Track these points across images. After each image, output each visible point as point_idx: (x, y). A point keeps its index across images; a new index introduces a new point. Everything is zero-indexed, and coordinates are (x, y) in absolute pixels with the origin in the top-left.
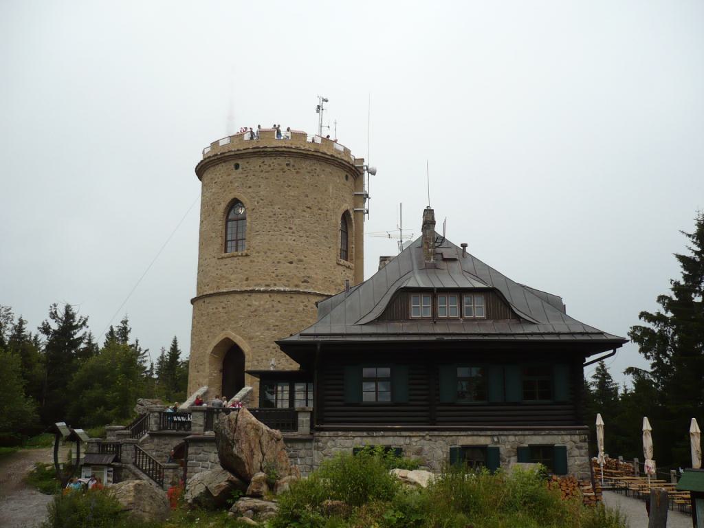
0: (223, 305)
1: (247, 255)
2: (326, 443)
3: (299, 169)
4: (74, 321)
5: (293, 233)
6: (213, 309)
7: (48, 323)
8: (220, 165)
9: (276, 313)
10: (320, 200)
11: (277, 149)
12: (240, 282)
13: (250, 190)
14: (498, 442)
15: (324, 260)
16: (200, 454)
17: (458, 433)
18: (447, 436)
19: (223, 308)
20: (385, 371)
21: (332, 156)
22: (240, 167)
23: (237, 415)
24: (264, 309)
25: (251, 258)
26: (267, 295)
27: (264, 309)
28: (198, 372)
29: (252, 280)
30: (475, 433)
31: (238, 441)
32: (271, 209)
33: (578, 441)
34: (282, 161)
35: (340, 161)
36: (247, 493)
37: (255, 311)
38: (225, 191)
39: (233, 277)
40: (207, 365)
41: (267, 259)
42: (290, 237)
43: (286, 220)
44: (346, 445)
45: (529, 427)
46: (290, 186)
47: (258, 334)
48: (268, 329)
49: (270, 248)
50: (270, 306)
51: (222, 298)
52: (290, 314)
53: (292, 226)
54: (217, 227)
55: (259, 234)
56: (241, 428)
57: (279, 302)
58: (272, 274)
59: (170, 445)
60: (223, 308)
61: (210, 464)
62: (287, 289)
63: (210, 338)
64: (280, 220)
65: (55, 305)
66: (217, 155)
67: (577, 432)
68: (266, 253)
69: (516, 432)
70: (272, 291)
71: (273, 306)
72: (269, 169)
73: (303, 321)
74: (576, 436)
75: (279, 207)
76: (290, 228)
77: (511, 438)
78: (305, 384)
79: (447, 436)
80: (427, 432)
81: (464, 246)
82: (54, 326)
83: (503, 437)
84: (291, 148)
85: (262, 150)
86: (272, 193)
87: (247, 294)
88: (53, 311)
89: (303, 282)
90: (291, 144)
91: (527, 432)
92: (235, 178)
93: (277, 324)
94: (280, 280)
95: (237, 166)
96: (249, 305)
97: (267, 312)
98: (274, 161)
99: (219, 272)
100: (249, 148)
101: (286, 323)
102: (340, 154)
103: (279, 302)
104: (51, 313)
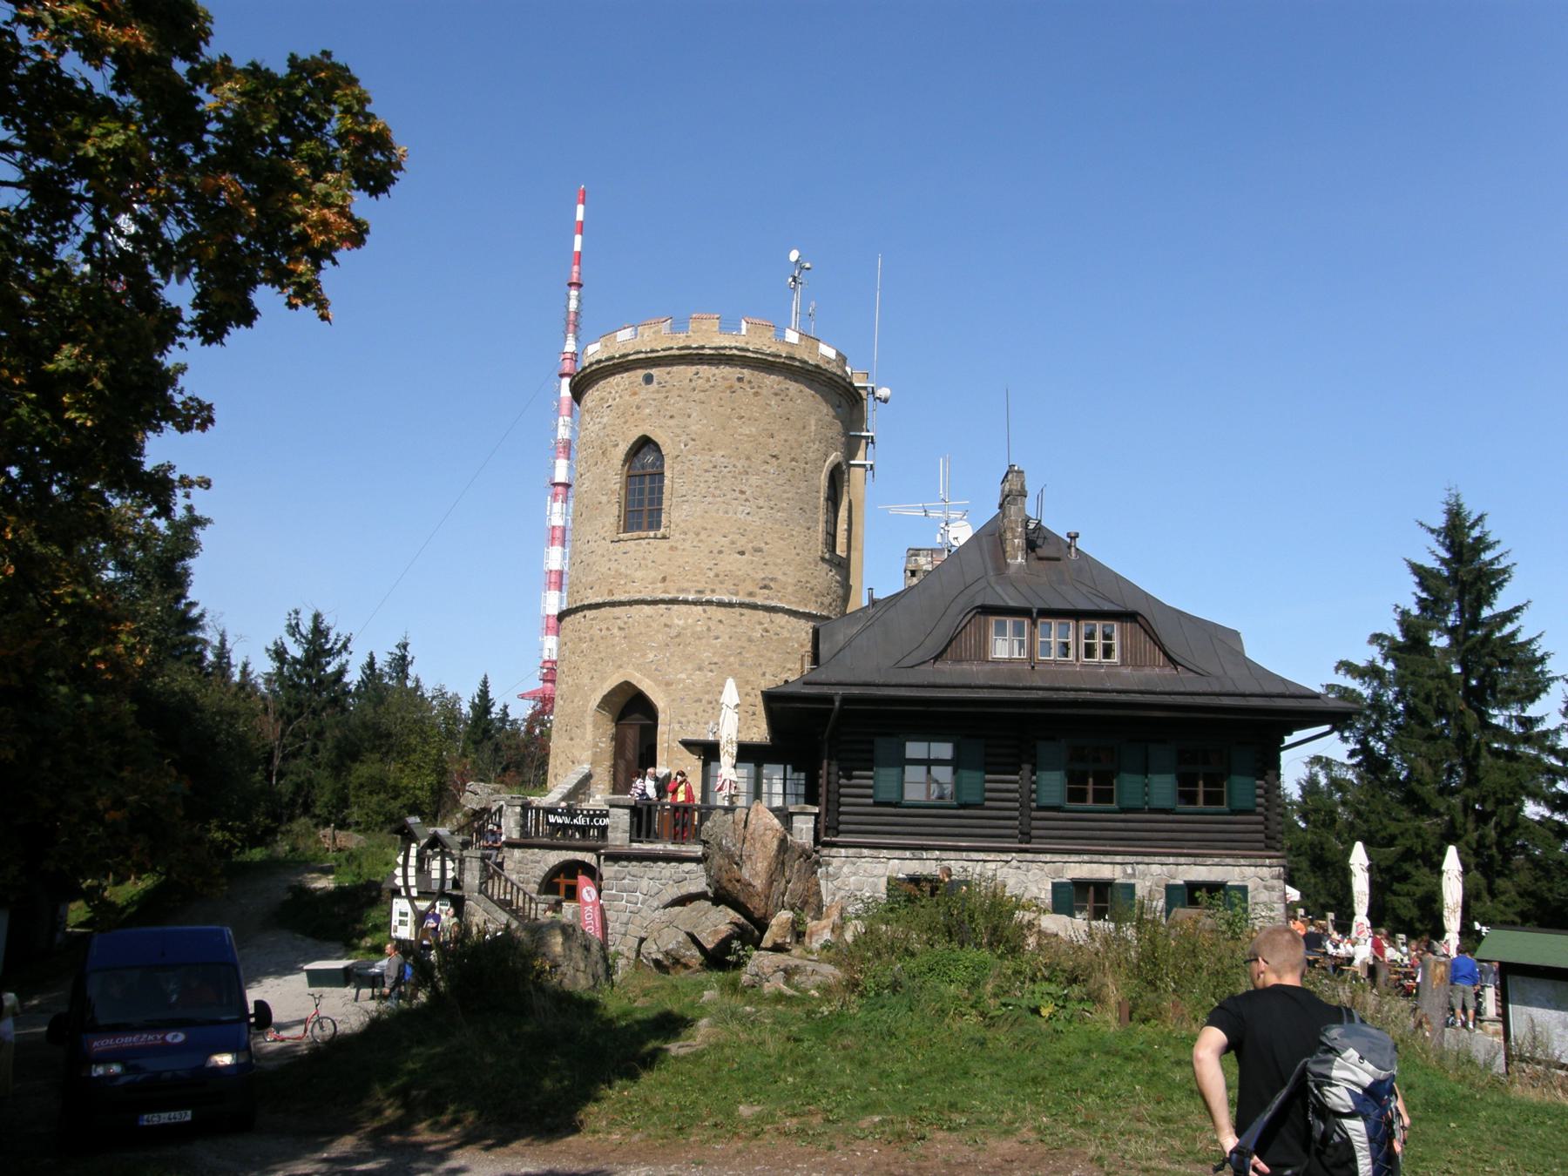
1: (664, 537)
2: (841, 868)
3: (759, 387)
4: (327, 642)
5: (747, 500)
6: (601, 630)
7: (283, 644)
10: (795, 445)
11: (723, 352)
12: (651, 584)
13: (672, 422)
14: (1133, 875)
15: (798, 551)
16: (624, 878)
17: (1066, 858)
18: (1046, 863)
19: (620, 629)
20: (944, 750)
21: (817, 366)
22: (655, 381)
23: (747, 815)
27: (693, 633)
28: (571, 739)
30: (1096, 858)
31: (749, 857)
32: (707, 458)
33: (1268, 877)
35: (829, 375)
36: (762, 945)
37: (678, 635)
38: (625, 422)
39: (639, 574)
40: (589, 728)
42: (741, 508)
43: (735, 478)
44: (875, 873)
45: (1185, 851)
47: (683, 676)
48: (700, 669)
51: (617, 611)
52: (739, 643)
53: (745, 488)
54: (610, 486)
56: (756, 836)
59: (542, 864)
60: (620, 629)
61: (641, 897)
62: (734, 599)
64: (724, 477)
65: (297, 613)
66: (613, 358)
67: (1267, 861)
68: (698, 534)
69: (1164, 859)
70: (709, 603)
71: (709, 629)
72: (707, 386)
73: (762, 656)
74: (1264, 868)
75: (722, 453)
76: (742, 492)
77: (1156, 869)
78: (782, 766)
79: (1046, 863)
80: (1014, 855)
81: (1074, 537)
82: (295, 651)
83: (1140, 866)
84: (748, 350)
85: (695, 352)
86: (712, 428)
87: (664, 606)
88: (294, 622)
90: (747, 343)
91: (1182, 860)
92: (644, 400)
93: (715, 660)
94: (722, 582)
95: (649, 379)
96: (666, 625)
97: (699, 638)
100: (671, 348)
102: (828, 363)
103: (720, 621)
104: (290, 626)
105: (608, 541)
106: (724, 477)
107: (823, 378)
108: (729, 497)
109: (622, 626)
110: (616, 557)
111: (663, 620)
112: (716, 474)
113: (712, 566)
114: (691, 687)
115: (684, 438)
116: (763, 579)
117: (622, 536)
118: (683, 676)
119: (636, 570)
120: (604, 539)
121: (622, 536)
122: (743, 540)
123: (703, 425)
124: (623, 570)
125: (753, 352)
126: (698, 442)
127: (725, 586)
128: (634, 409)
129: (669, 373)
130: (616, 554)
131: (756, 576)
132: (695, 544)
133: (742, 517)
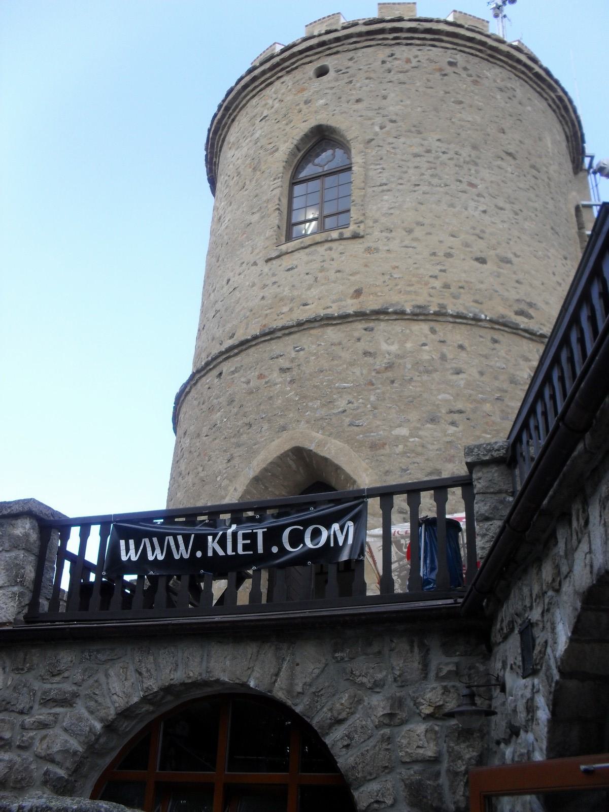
0: (283, 363)
1: (356, 236)
5: (479, 195)
6: (248, 382)
8: (282, 80)
9: (455, 377)
12: (334, 302)
13: (359, 106)
24: (416, 364)
25: (368, 242)
26: (424, 327)
27: (416, 364)
29: (375, 294)
34: (439, 55)
35: (561, 94)
37: (390, 367)
39: (315, 292)
41: (414, 244)
42: (472, 204)
43: (460, 166)
46: (461, 103)
47: (404, 431)
48: (433, 420)
49: (421, 219)
50: (436, 356)
51: (276, 347)
52: (497, 383)
53: (474, 181)
55: (389, 190)
57: (461, 347)
58: (432, 280)
59: (80, 709)
60: (283, 370)
63: (236, 461)
64: (443, 164)
68: (410, 231)
71: (443, 358)
72: (408, 66)
75: (438, 137)
76: (472, 185)
86: (419, 109)
87: (360, 326)
89: (517, 313)
93: (459, 406)
95: (322, 72)
96: (366, 353)
98: (419, 53)
99: (268, 292)
101: (487, 407)
103: (461, 347)
105: (261, 263)
106: (443, 164)
107: (553, 95)
108: (453, 187)
109: (287, 365)
110: (274, 279)
111: (362, 346)
112: (431, 159)
113: (437, 273)
114: (420, 449)
115: (378, 120)
116: (518, 300)
117: (284, 248)
118: (404, 431)
119: (309, 288)
120: (255, 264)
121: (284, 248)
122: (481, 244)
123: (406, 106)
124: (286, 292)
125: (468, 29)
126: (400, 124)
127: (460, 301)
128: (302, 106)
129: (351, 59)
130: (274, 275)
131: (506, 294)
132: (406, 243)
133: (476, 214)
